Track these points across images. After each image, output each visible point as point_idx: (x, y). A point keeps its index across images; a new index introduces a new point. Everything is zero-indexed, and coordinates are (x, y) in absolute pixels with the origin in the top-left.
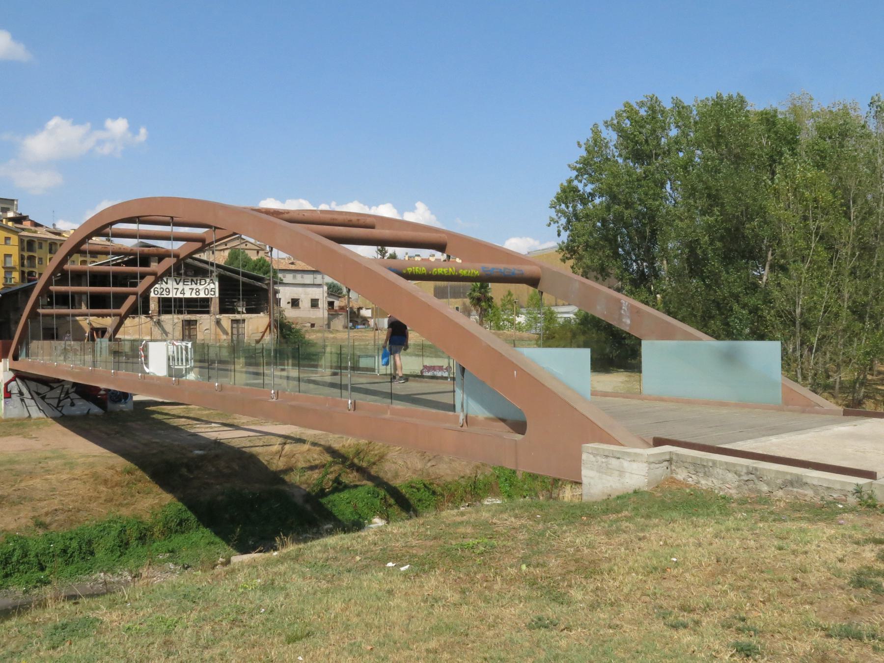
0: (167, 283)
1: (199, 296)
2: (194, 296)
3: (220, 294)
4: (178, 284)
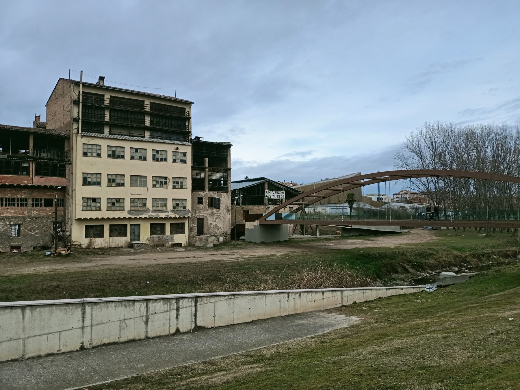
2: (278, 198)
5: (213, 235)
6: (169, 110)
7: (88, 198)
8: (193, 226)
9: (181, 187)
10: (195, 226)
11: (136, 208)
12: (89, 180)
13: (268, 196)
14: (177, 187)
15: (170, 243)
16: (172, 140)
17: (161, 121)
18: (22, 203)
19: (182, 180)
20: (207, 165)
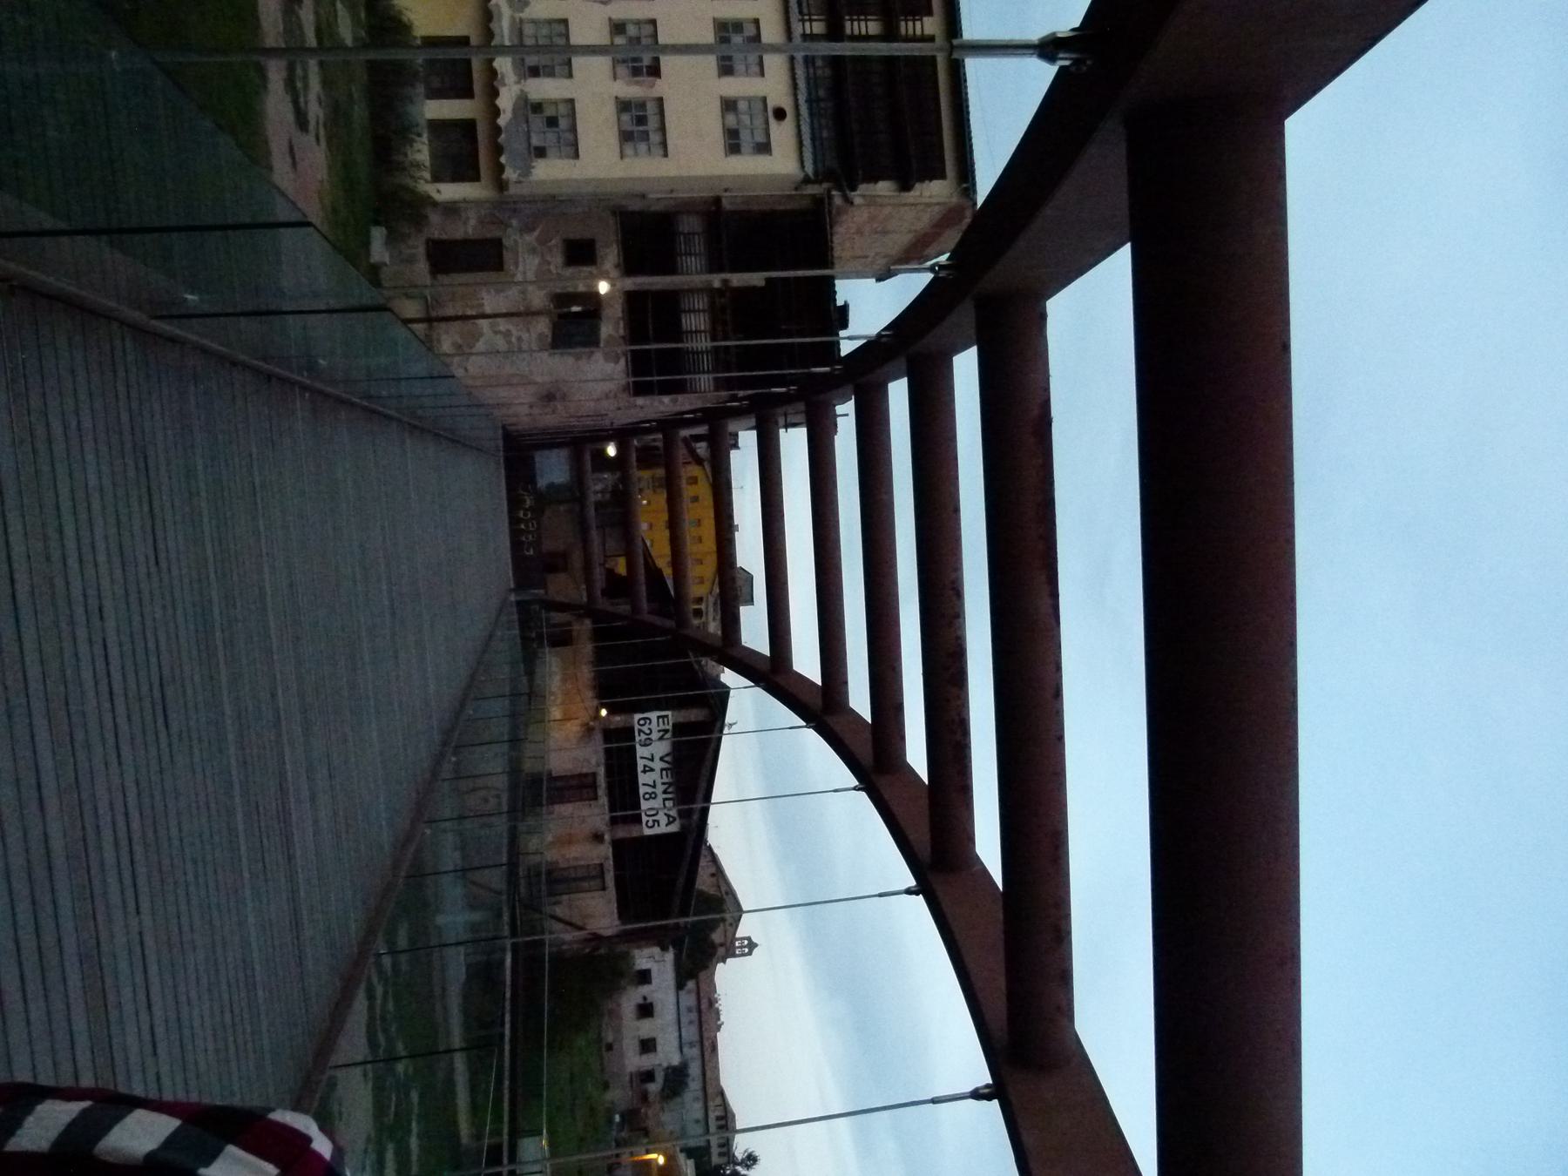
0: (661, 738)
1: (642, 801)
2: (642, 790)
3: (650, 837)
4: (662, 759)
8: (468, 218)
9: (626, 137)
10: (468, 228)
13: (645, 729)
14: (626, 117)
19: (655, 138)
20: (738, 279)
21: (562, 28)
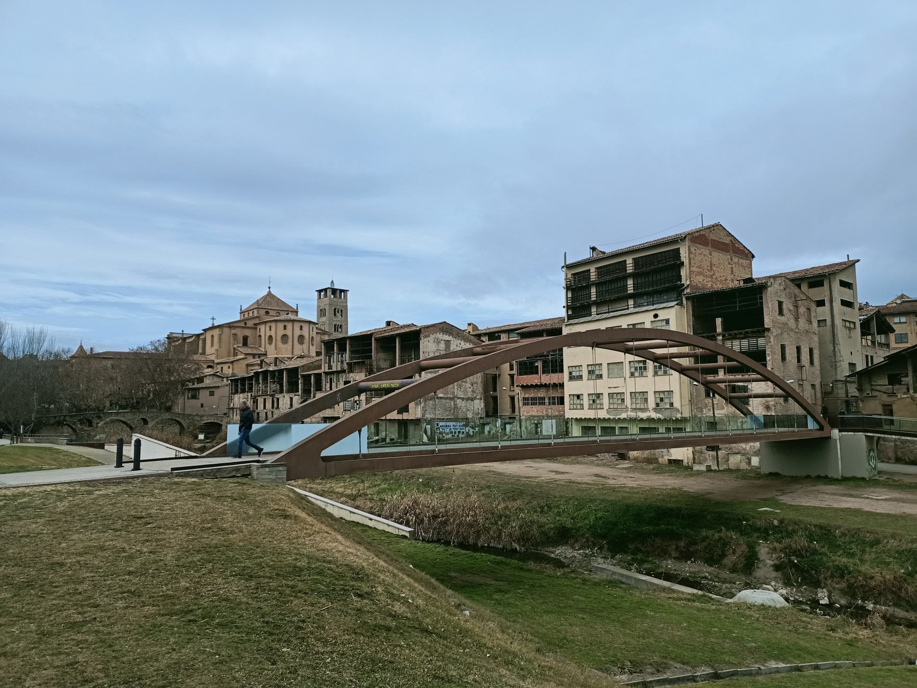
5: (738, 453)
6: (660, 259)
7: (573, 395)
11: (615, 406)
12: (574, 374)
14: (659, 373)
15: (666, 458)
16: (656, 304)
17: (647, 279)
18: (541, 402)
20: (719, 329)
21: (633, 394)
